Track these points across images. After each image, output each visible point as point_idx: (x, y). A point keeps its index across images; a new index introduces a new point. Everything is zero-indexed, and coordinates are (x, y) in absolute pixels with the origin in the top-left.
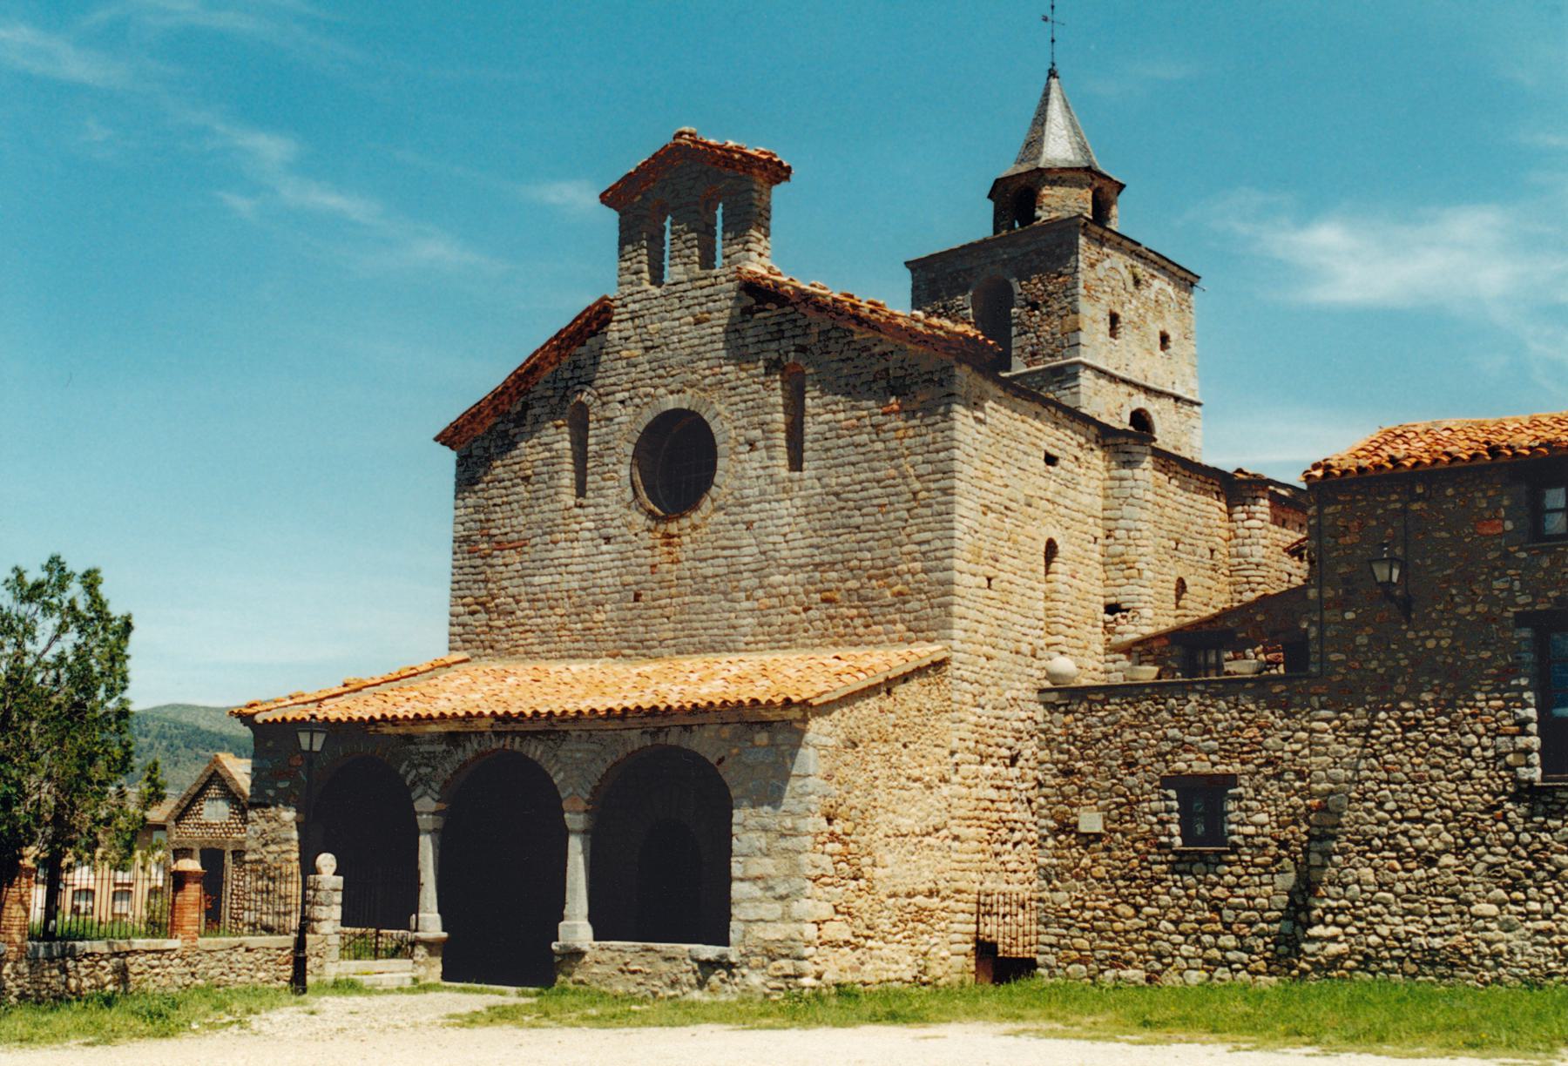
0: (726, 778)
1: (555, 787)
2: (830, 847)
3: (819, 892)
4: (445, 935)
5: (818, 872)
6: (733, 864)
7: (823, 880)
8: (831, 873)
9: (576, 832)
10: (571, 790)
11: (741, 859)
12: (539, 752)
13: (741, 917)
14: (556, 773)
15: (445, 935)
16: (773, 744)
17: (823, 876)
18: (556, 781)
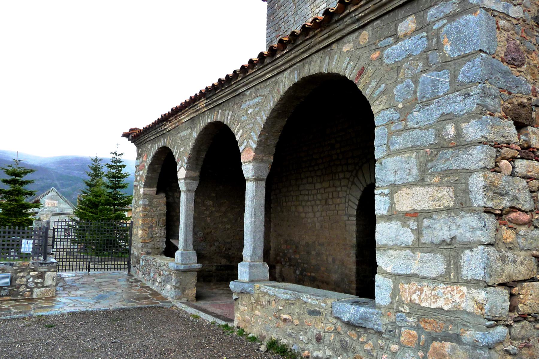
0: (367, 93)
1: (237, 142)
2: (522, 166)
3: (508, 235)
4: (199, 266)
5: (506, 203)
6: (377, 197)
7: (513, 215)
8: (527, 206)
9: (250, 180)
10: (245, 144)
11: (386, 191)
12: (229, 117)
13: (389, 269)
14: (238, 132)
15: (199, 266)
16: (422, 26)
17: (513, 209)
18: (237, 138)
